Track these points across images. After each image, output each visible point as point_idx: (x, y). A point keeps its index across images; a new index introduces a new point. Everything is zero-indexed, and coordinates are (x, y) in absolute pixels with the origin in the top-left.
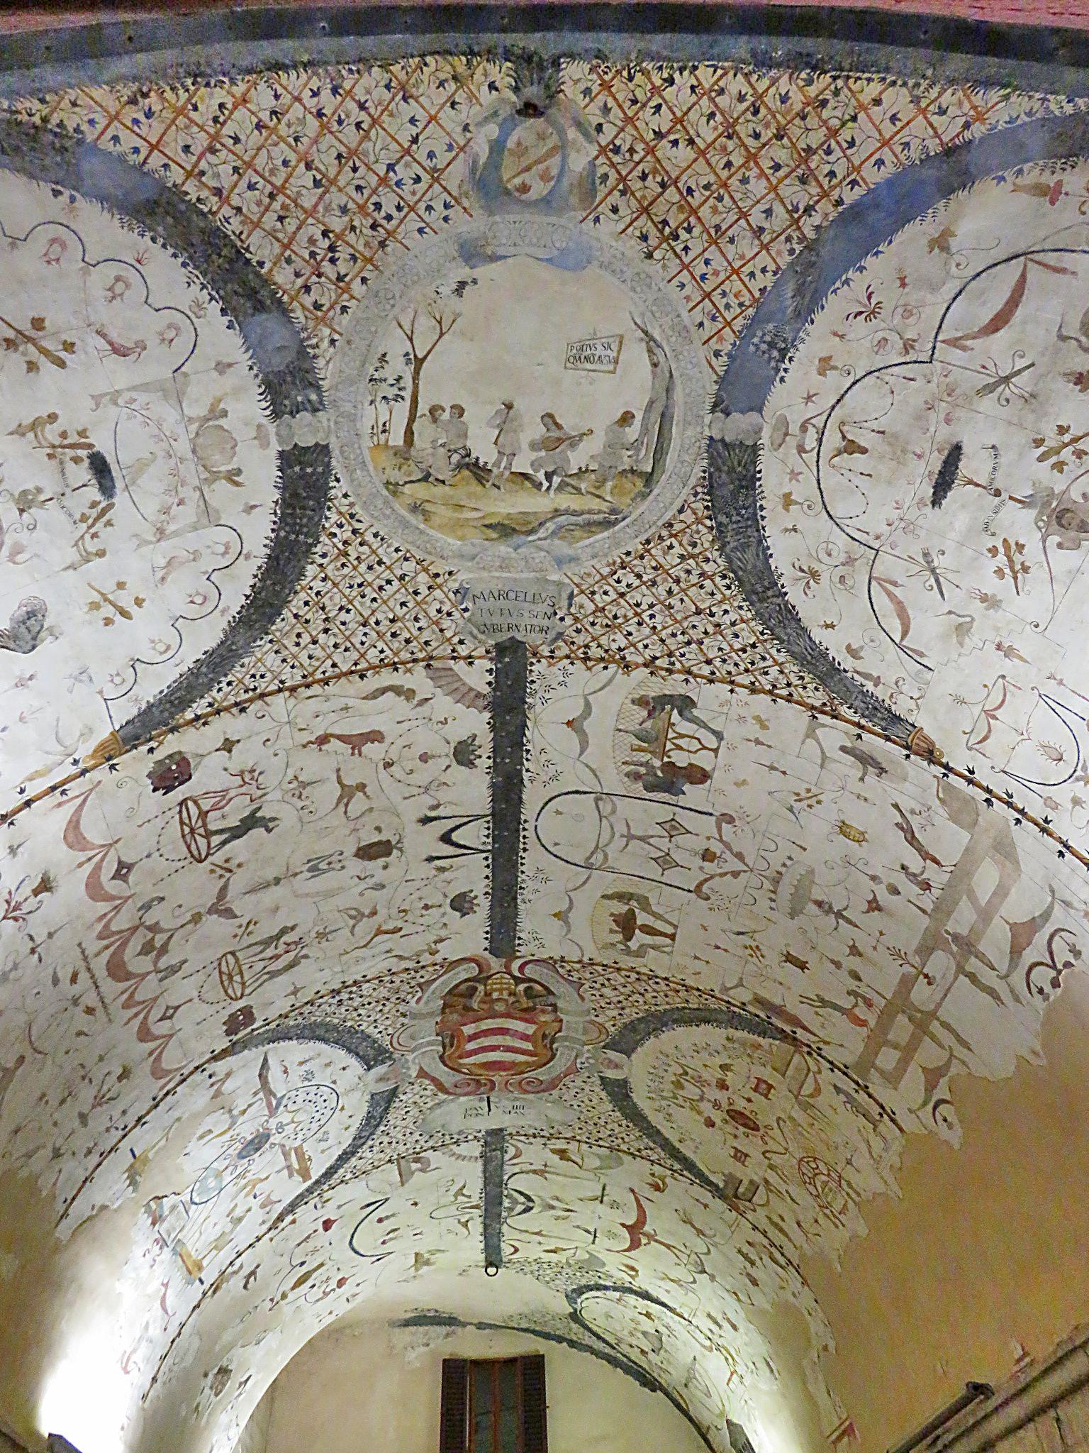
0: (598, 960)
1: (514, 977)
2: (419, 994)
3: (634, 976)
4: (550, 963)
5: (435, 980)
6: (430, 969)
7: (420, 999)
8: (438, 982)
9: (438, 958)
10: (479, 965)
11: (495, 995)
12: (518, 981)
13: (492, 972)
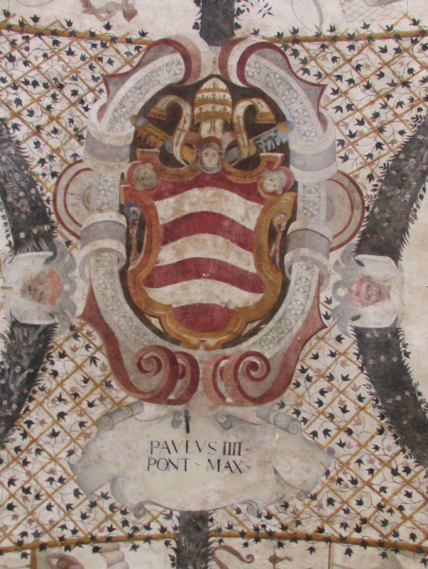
0: (341, 30)
1: (231, 87)
2: (104, 98)
3: (391, 44)
4: (280, 46)
5: (127, 75)
6: (123, 48)
7: (103, 109)
8: (130, 83)
9: (132, 29)
10: (187, 58)
11: (205, 130)
12: (238, 93)
13: (204, 75)
